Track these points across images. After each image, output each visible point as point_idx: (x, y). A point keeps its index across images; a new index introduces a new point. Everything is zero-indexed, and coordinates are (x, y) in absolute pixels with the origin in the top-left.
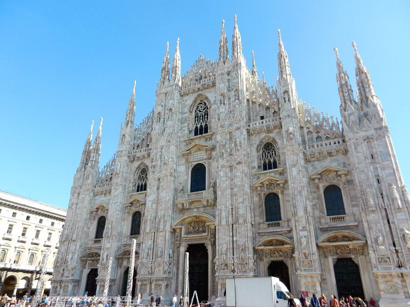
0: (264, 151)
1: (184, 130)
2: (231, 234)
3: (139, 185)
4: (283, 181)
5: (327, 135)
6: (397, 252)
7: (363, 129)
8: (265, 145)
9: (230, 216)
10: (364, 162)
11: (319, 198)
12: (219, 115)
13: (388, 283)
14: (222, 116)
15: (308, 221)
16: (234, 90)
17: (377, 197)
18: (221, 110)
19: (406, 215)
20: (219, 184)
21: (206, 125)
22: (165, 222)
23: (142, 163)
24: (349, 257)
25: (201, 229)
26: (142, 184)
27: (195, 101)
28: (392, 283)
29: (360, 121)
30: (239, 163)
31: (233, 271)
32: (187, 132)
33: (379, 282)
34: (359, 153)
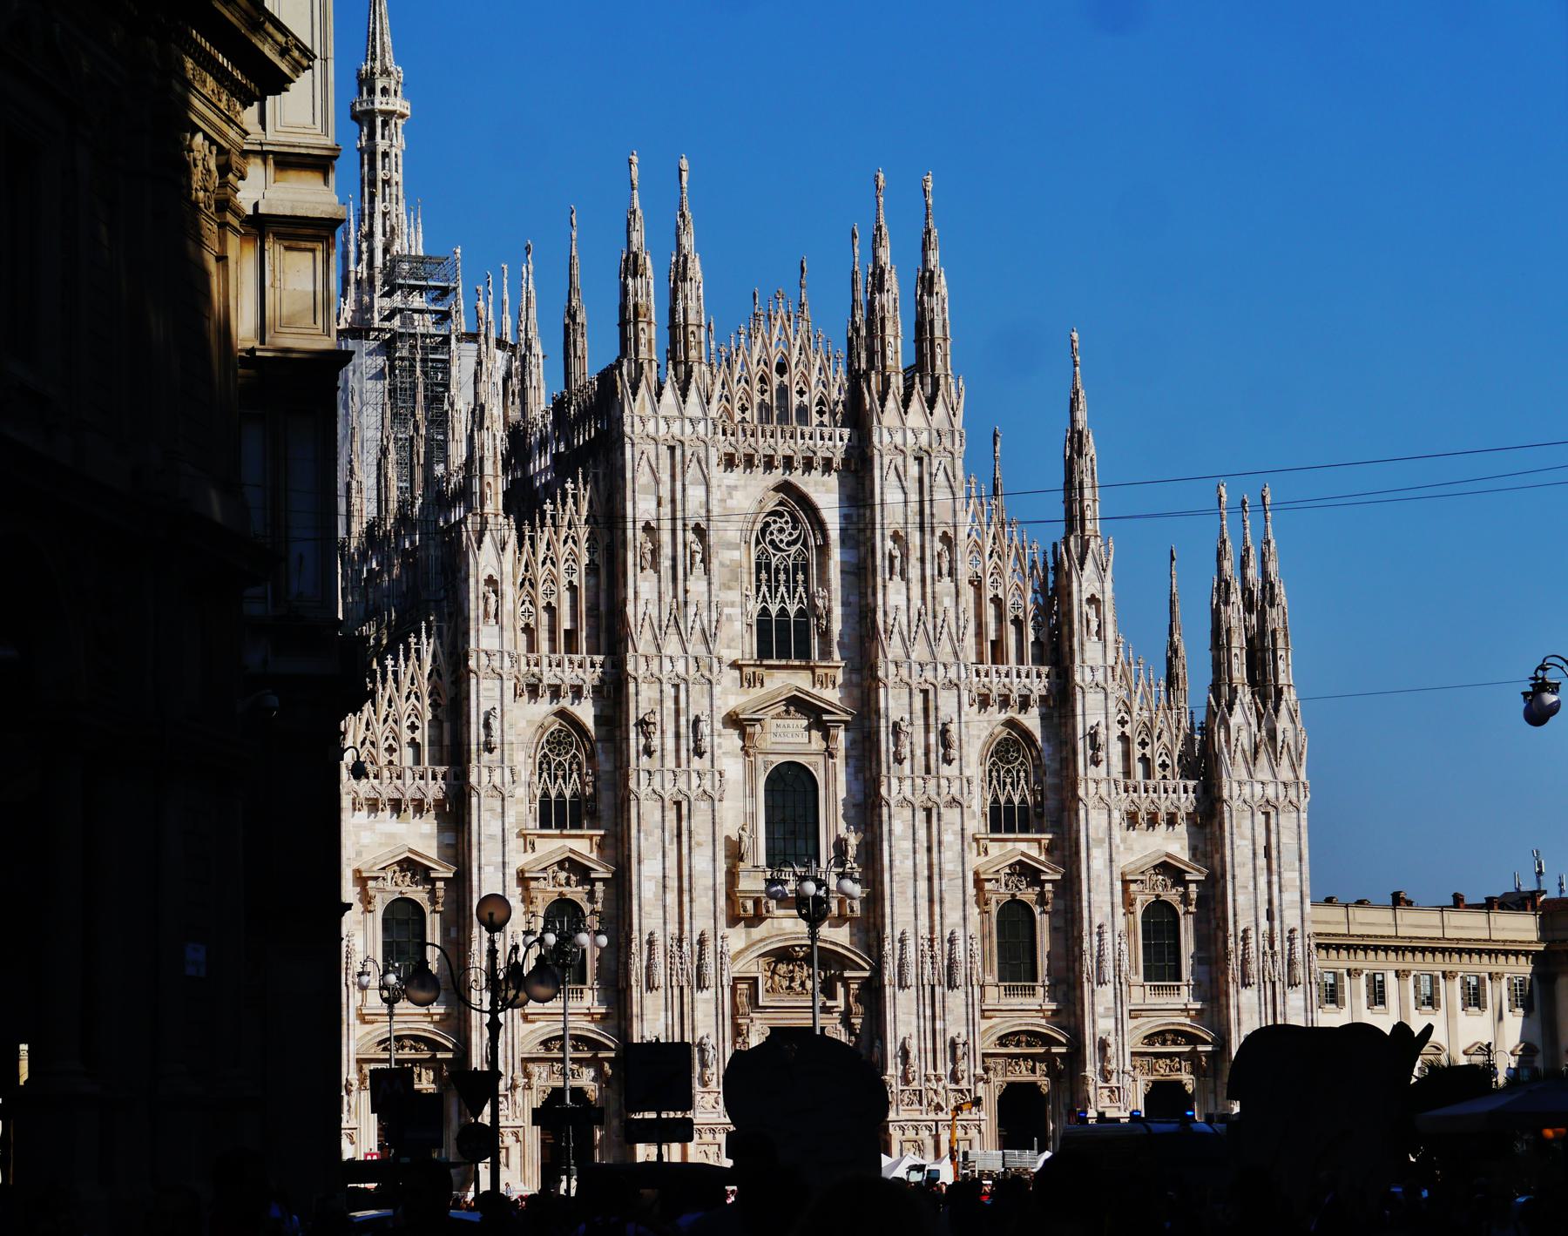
0: (994, 764)
1: (729, 618)
2: (928, 1012)
3: (546, 794)
4: (1058, 877)
9: (928, 960)
10: (1251, 866)
11: (1130, 931)
16: (938, 533)
17: (1264, 953)
21: (800, 612)
22: (720, 955)
24: (1175, 1077)
25: (809, 984)
26: (561, 795)
30: (954, 802)
31: (939, 1108)
32: (738, 626)
34: (1242, 837)
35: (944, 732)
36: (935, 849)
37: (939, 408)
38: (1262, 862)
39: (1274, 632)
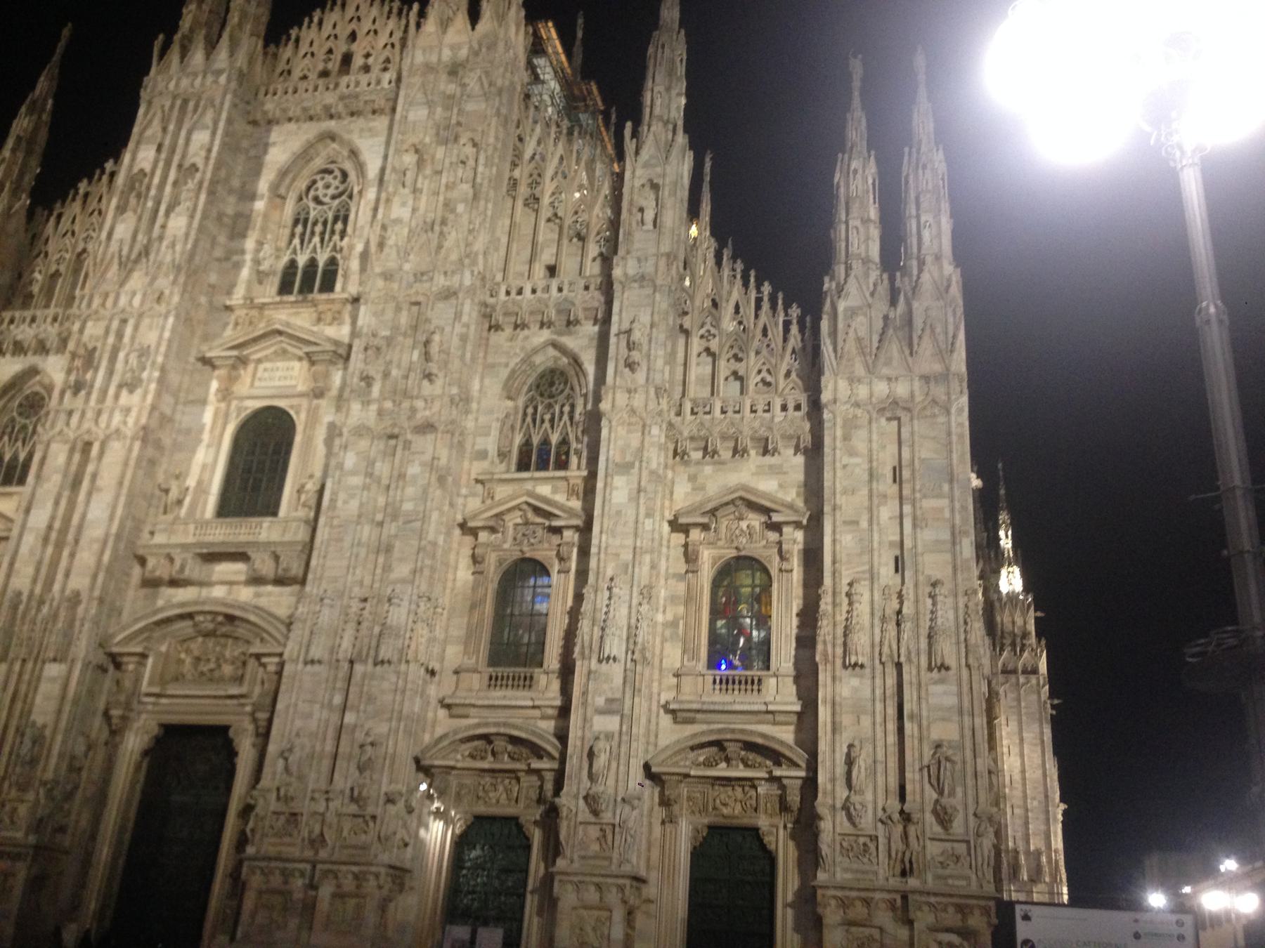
0: (532, 399)
2: (338, 699)
4: (578, 522)
5: (764, 374)
6: (906, 817)
7: (885, 371)
8: (542, 376)
10: (865, 492)
11: (690, 599)
12: (384, 227)
13: (854, 929)
14: (396, 237)
15: (630, 681)
17: (884, 619)
18: (400, 211)
19: (960, 694)
20: (333, 501)
21: (332, 262)
23: (33, 371)
24: (746, 821)
25: (227, 669)
27: (304, 156)
28: (867, 931)
29: (880, 341)
30: (427, 427)
33: (826, 921)
34: (852, 453)
35: (427, 343)
36: (393, 486)
37: (484, 25)
38: (886, 486)
39: (917, 199)
